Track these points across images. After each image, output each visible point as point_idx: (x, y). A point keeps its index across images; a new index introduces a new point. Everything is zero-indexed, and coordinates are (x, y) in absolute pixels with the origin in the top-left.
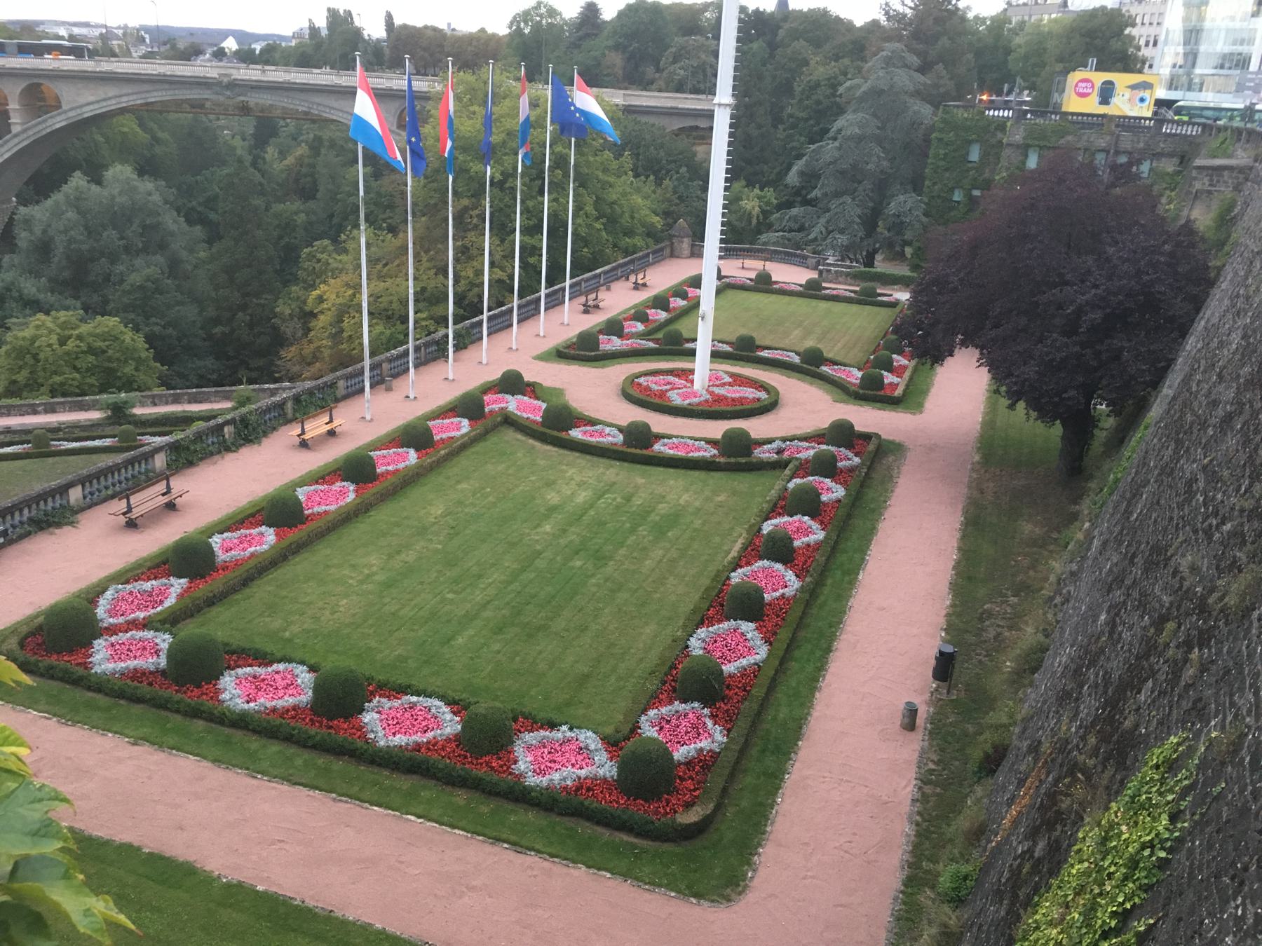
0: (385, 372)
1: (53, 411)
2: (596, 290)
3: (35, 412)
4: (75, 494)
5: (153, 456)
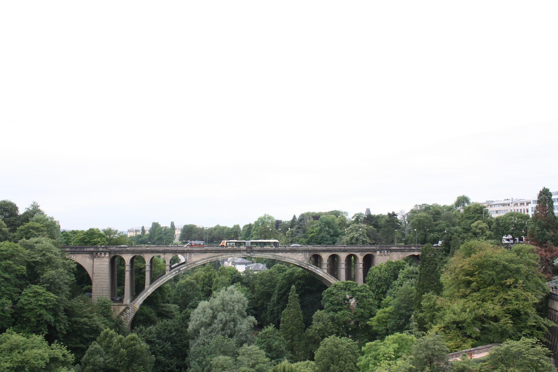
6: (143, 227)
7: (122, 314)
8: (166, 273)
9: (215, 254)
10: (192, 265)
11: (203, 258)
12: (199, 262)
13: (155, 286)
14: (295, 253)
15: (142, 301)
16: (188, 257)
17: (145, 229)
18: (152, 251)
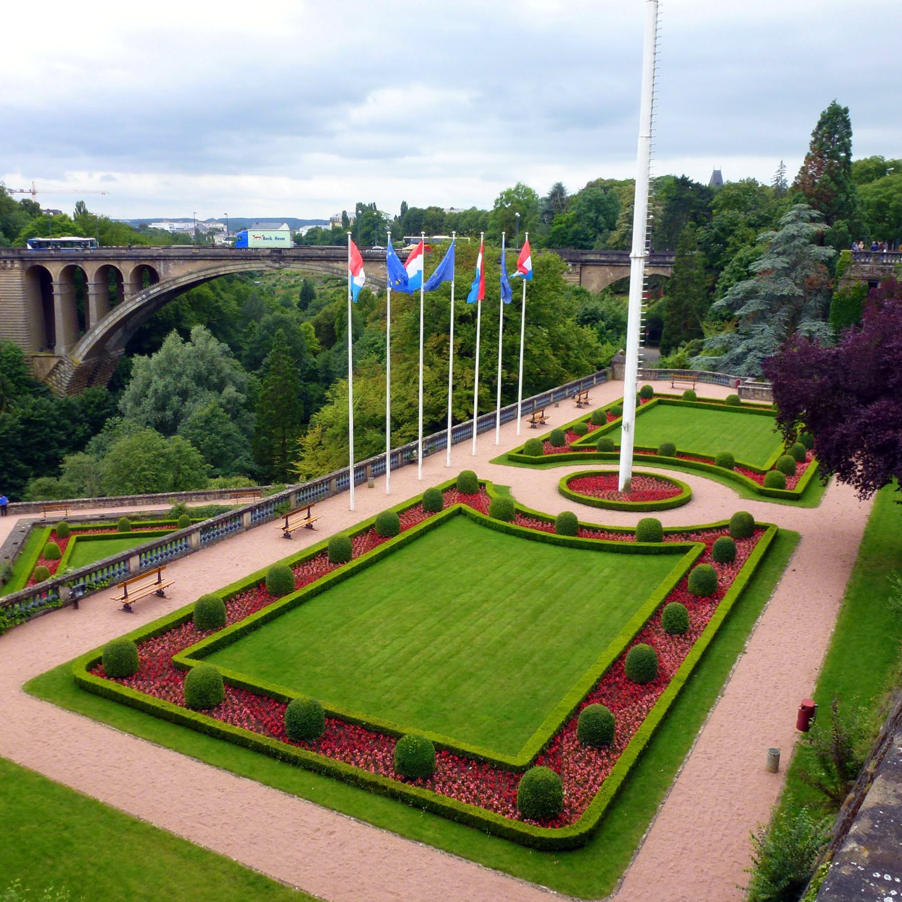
0: (369, 473)
1: (135, 504)
2: (542, 408)
3: (122, 505)
4: (135, 562)
5: (190, 535)
6: (344, 213)
7: (52, 373)
8: (125, 299)
10: (171, 283)
11: (190, 270)
12: (183, 279)
13: (106, 323)
14: (372, 264)
15: (87, 350)
16: (162, 268)
17: (349, 216)
18: (96, 257)
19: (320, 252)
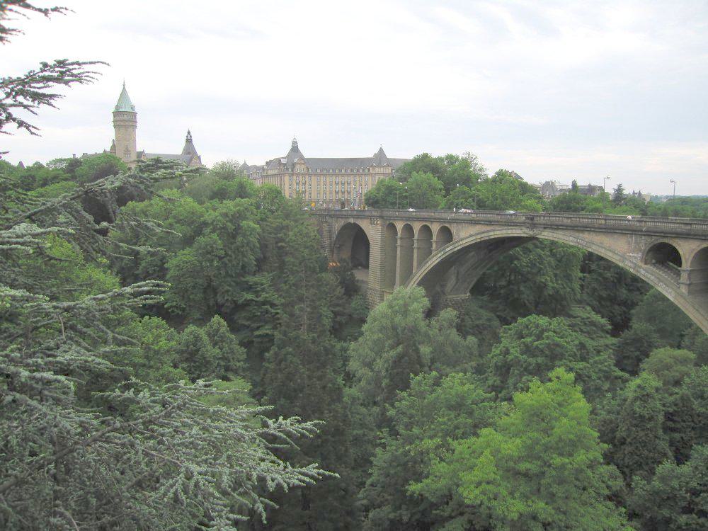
9: (486, 226)
12: (468, 240)
14: (616, 236)
19: (566, 220)
